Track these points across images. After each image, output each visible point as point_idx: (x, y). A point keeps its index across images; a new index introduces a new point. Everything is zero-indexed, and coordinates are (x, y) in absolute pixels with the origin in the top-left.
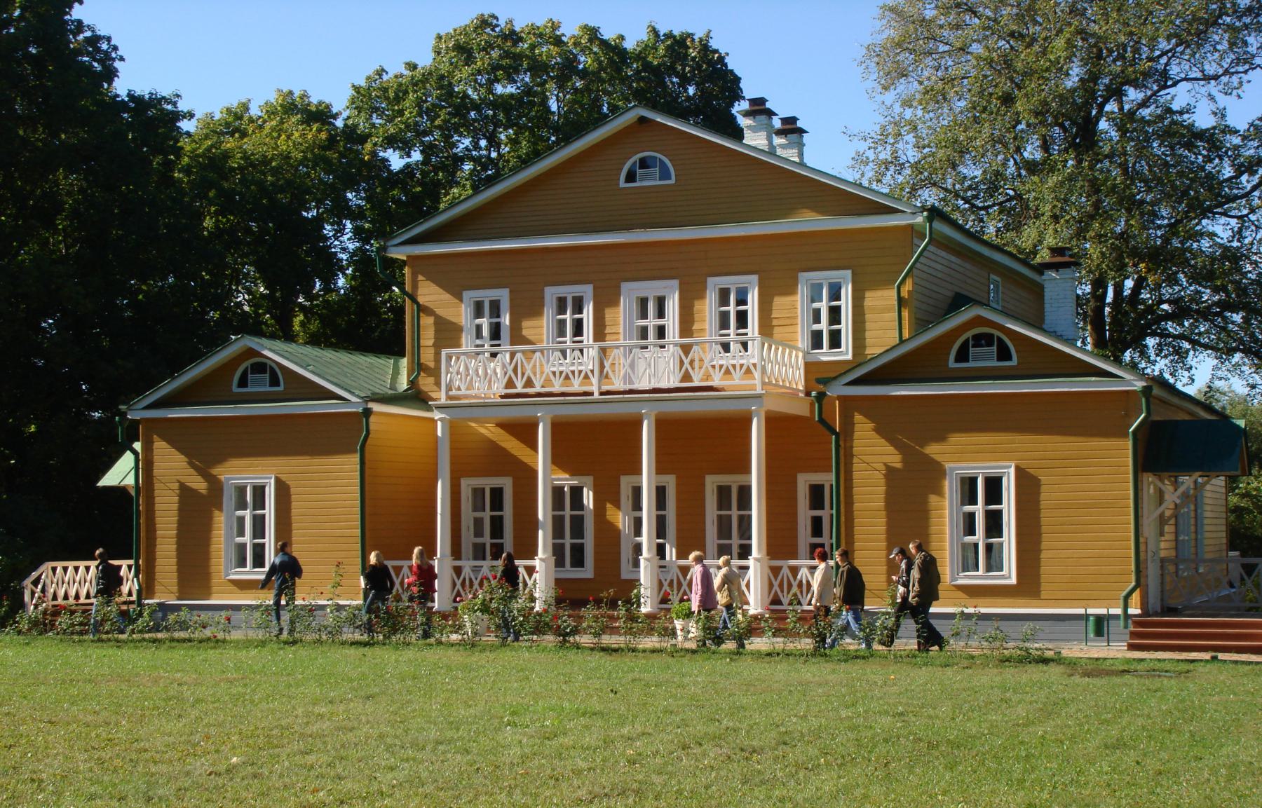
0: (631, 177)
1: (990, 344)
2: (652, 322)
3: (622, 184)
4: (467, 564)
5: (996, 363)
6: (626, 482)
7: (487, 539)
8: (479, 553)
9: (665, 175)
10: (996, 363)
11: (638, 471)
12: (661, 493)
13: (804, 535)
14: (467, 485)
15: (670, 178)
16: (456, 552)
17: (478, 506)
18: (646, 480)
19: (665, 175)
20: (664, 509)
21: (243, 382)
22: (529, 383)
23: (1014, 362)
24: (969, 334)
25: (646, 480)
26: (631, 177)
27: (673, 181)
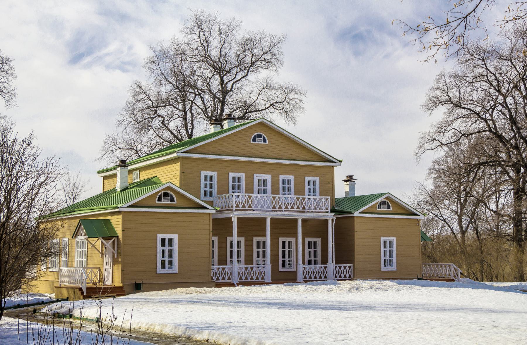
0: (254, 140)
1: (385, 204)
2: (262, 188)
4: (307, 266)
5: (170, 202)
6: (229, 239)
8: (310, 262)
9: (264, 141)
10: (170, 202)
12: (239, 242)
13: (307, 258)
14: (307, 239)
16: (304, 262)
19: (264, 141)
21: (160, 199)
22: (304, 208)
23: (175, 202)
24: (162, 192)
26: (254, 140)
27: (267, 143)
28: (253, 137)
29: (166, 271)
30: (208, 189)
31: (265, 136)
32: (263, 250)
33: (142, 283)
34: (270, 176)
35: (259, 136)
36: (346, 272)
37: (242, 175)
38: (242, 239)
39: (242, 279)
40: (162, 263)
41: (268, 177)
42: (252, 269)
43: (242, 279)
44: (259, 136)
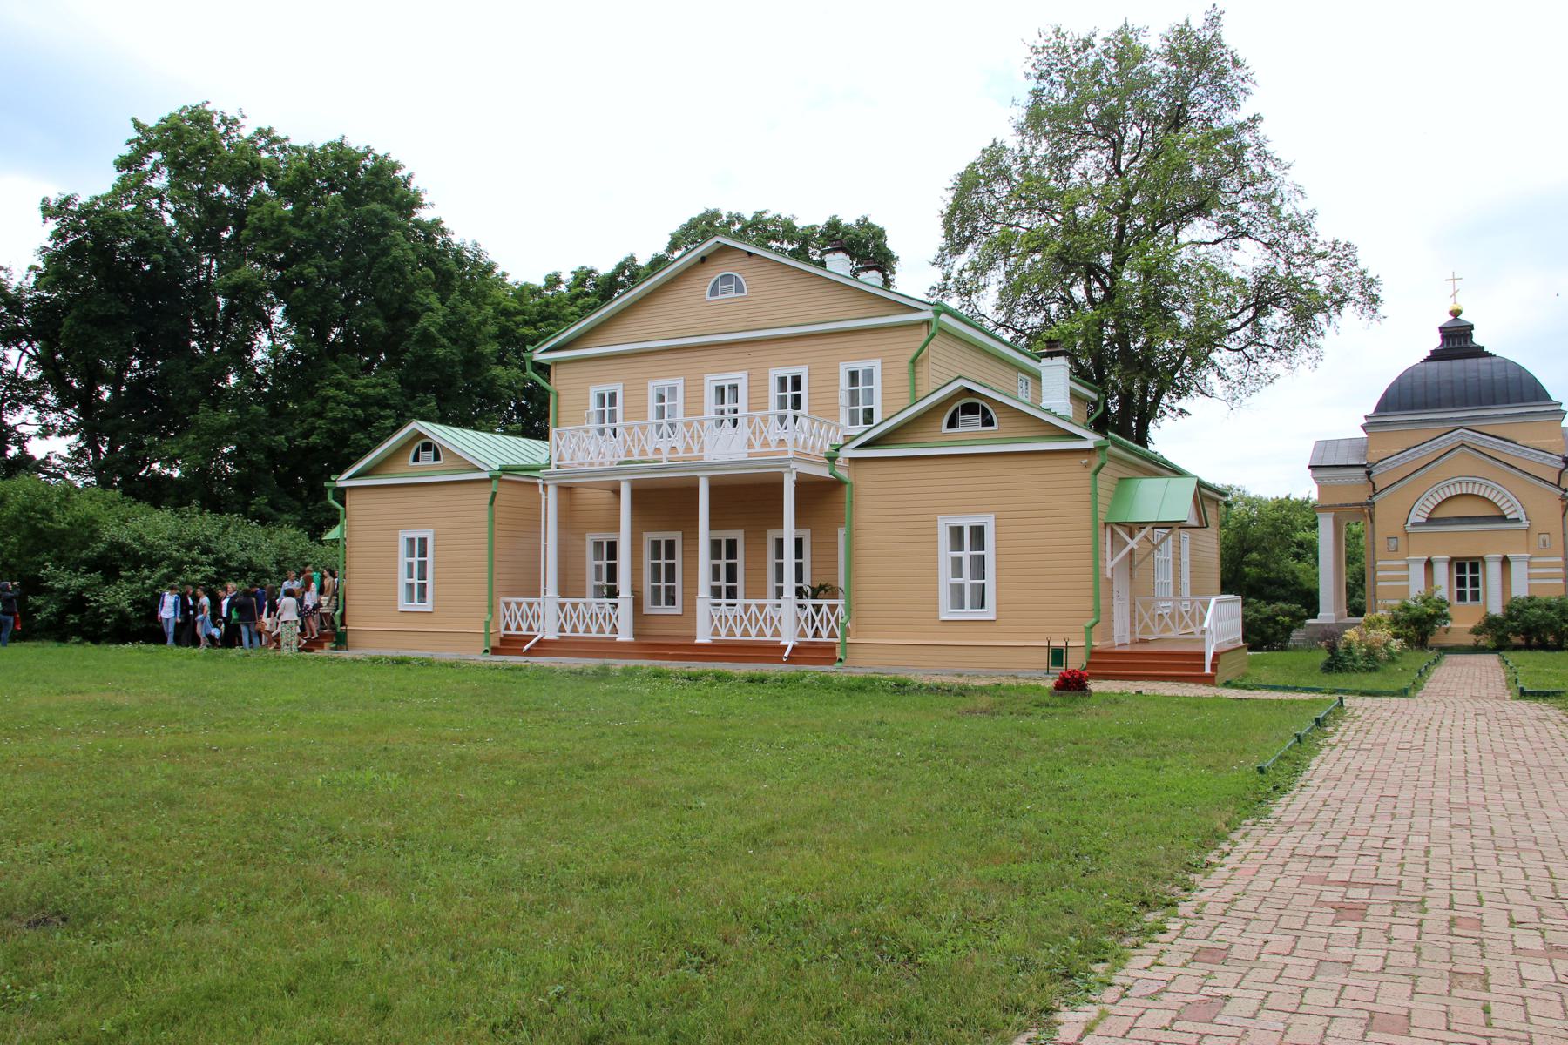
3: (708, 297)
7: (723, 583)
9: (739, 289)
11: (781, 526)
15: (743, 292)
17: (656, 554)
18: (789, 532)
20: (801, 558)
25: (789, 532)
26: (714, 292)
28: (710, 285)
29: (968, 613)
30: (790, 412)
31: (740, 277)
32: (727, 564)
33: (1067, 647)
34: (708, 378)
35: (727, 279)
36: (522, 617)
37: (679, 383)
38: (806, 534)
39: (510, 630)
40: (674, 598)
41: (741, 379)
42: (761, 608)
43: (510, 630)
44: (727, 279)
